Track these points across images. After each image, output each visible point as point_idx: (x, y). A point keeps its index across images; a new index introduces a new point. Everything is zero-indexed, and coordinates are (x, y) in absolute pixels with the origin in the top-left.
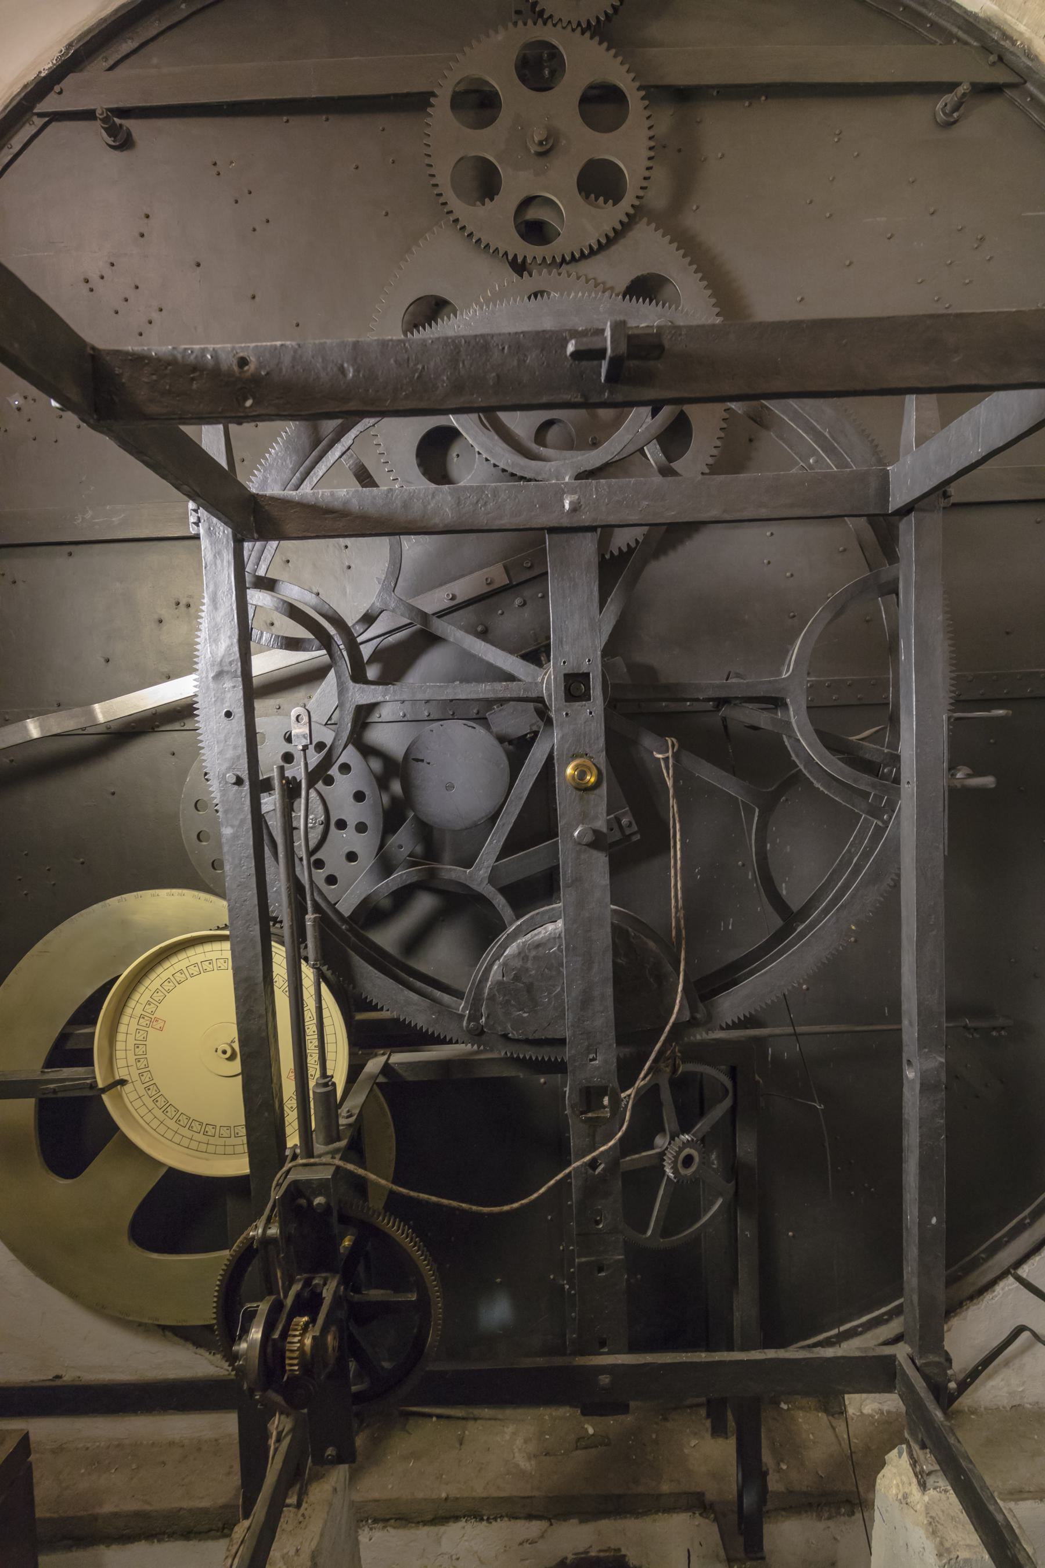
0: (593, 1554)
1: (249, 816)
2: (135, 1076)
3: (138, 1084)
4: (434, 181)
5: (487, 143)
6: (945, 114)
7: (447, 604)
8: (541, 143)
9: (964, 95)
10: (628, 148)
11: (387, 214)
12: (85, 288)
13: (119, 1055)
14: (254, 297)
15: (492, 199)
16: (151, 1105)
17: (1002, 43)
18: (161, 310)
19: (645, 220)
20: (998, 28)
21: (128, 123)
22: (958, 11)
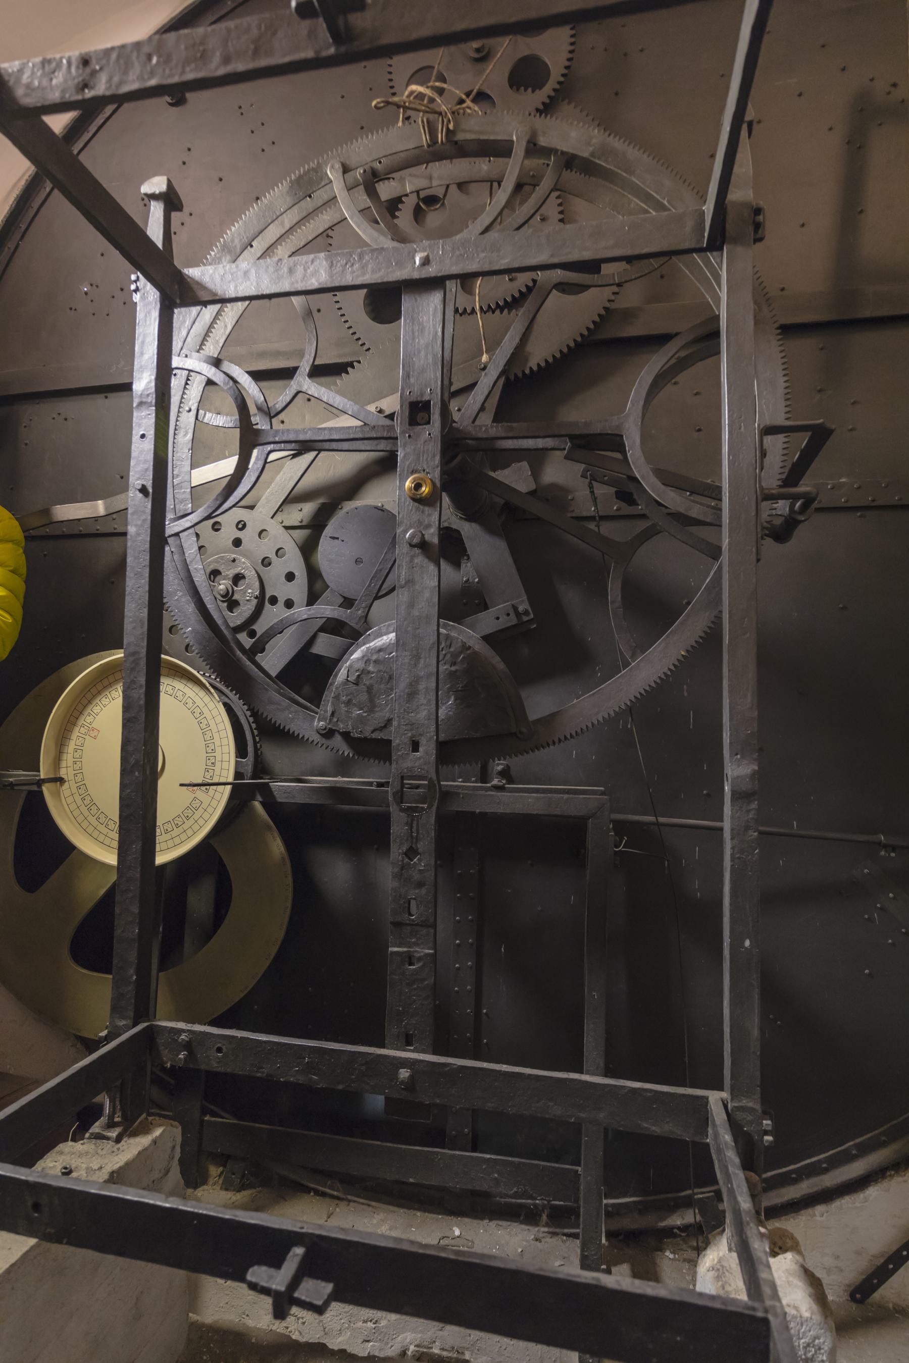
0: (436, 1351)
1: (149, 518)
2: (71, 777)
3: (72, 783)
16: (79, 802)
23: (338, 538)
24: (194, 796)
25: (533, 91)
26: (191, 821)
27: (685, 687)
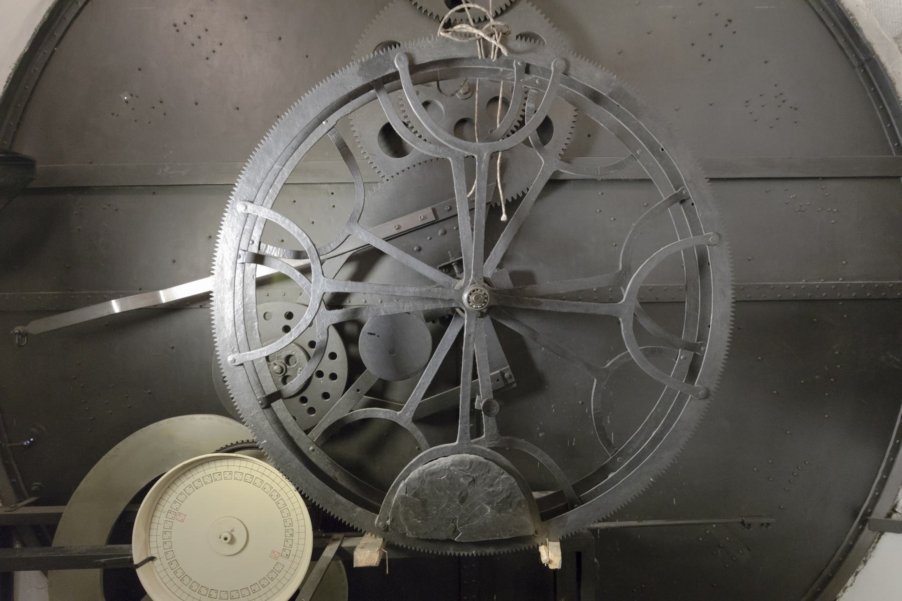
7: (394, 232)
12: (174, 29)
13: (153, 539)
14: (280, 39)
16: (172, 575)
26: (276, 581)
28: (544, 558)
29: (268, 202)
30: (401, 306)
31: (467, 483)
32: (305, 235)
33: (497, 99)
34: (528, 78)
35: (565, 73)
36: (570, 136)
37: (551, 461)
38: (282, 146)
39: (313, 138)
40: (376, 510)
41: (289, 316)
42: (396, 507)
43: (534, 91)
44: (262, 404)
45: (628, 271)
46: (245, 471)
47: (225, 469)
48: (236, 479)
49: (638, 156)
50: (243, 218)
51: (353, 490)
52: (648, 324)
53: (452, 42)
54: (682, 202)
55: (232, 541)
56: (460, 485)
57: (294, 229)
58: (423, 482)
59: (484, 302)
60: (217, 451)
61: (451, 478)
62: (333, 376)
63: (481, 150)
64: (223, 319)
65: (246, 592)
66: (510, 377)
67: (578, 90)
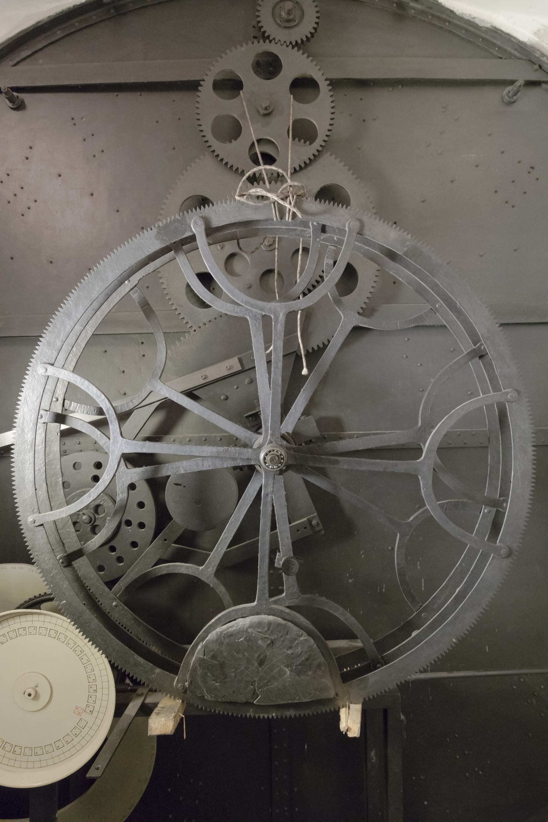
4: (201, 128)
5: (231, 107)
6: (508, 96)
8: (266, 109)
9: (520, 86)
10: (319, 112)
11: (174, 149)
15: (235, 140)
17: (541, 58)
18: (36, 201)
19: (329, 153)
20: (538, 50)
21: (22, 96)
22: (514, 41)
23: (180, 485)
24: (80, 717)
25: (305, 142)
27: (418, 563)
28: (343, 726)
29: (72, 361)
30: (201, 464)
31: (265, 646)
32: (103, 397)
33: (298, 250)
34: (324, 236)
35: (360, 233)
36: (374, 285)
37: (353, 619)
38: (81, 309)
39: (116, 298)
40: (174, 670)
41: (98, 466)
42: (194, 670)
43: (332, 248)
44: (62, 563)
45: (428, 426)
46: (50, 626)
47: (30, 624)
48: (40, 634)
49: (437, 310)
50: (43, 381)
51: (155, 649)
52: (447, 480)
53: (248, 206)
54: (481, 357)
55: (37, 697)
56: (258, 647)
57: (93, 391)
58: (221, 644)
59: (280, 463)
60: (18, 608)
61: (249, 639)
62: (142, 525)
63: (278, 310)
64: (23, 479)
65: (49, 748)
66: (318, 524)
67: (374, 248)
